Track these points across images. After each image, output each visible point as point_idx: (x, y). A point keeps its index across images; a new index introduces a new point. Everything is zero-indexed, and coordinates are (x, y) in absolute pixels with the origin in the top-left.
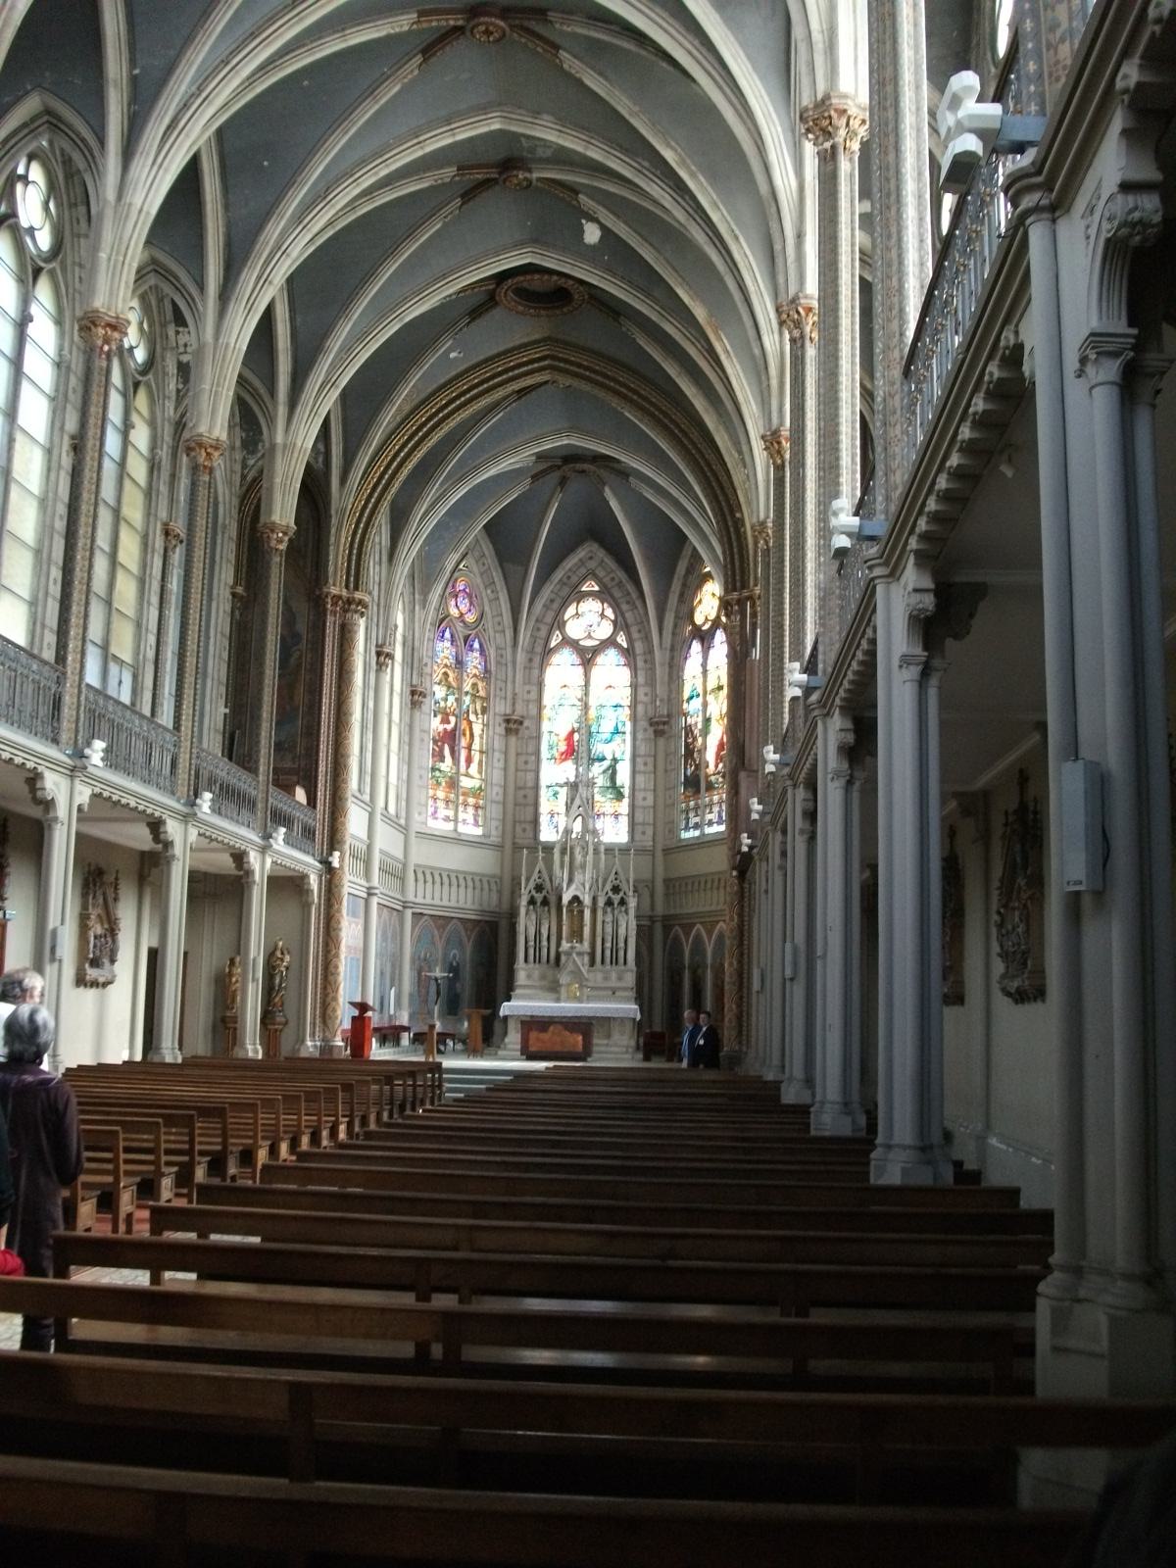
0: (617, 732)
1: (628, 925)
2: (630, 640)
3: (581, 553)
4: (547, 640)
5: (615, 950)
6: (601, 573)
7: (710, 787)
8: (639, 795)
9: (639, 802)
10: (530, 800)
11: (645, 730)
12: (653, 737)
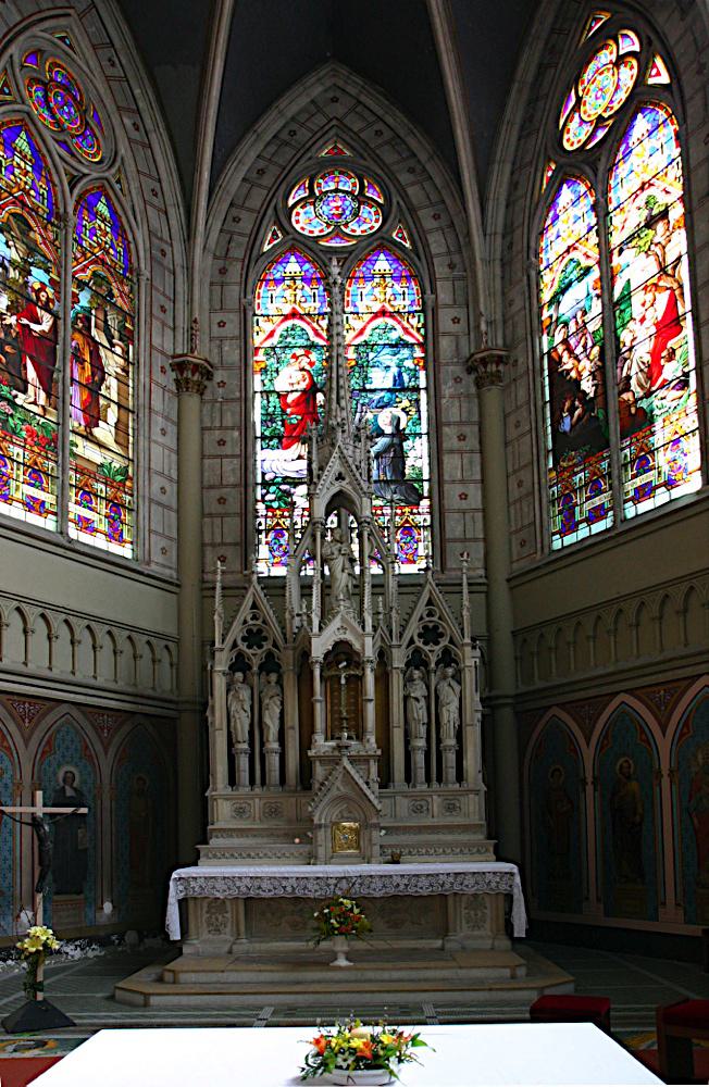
0: (399, 387)
2: (419, 237)
3: (313, 88)
4: (255, 238)
8: (452, 492)
10: (234, 505)
11: (457, 380)
12: (473, 390)
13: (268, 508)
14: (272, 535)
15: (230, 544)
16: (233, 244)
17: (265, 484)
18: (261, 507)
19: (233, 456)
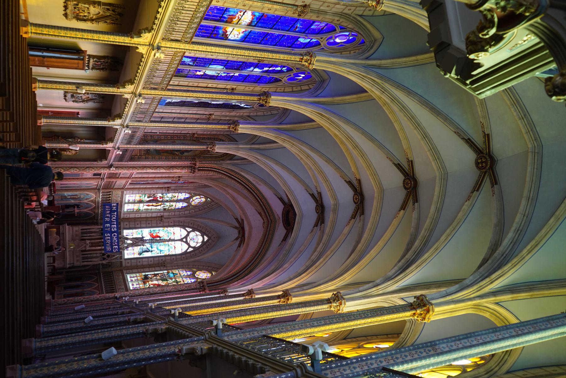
1: (97, 261)
5: (87, 258)
6: (210, 241)
7: (145, 283)
9: (139, 260)
10: (137, 226)
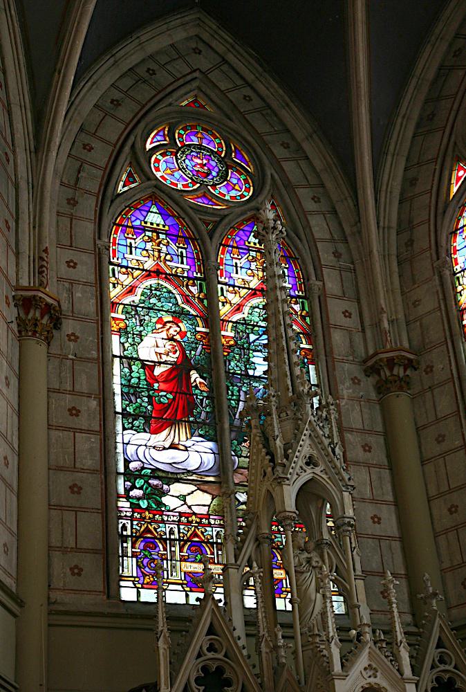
13: (135, 507)
14: (140, 544)
15: (86, 551)
16: (82, 174)
17: (129, 475)
18: (124, 504)
19: (89, 431)
